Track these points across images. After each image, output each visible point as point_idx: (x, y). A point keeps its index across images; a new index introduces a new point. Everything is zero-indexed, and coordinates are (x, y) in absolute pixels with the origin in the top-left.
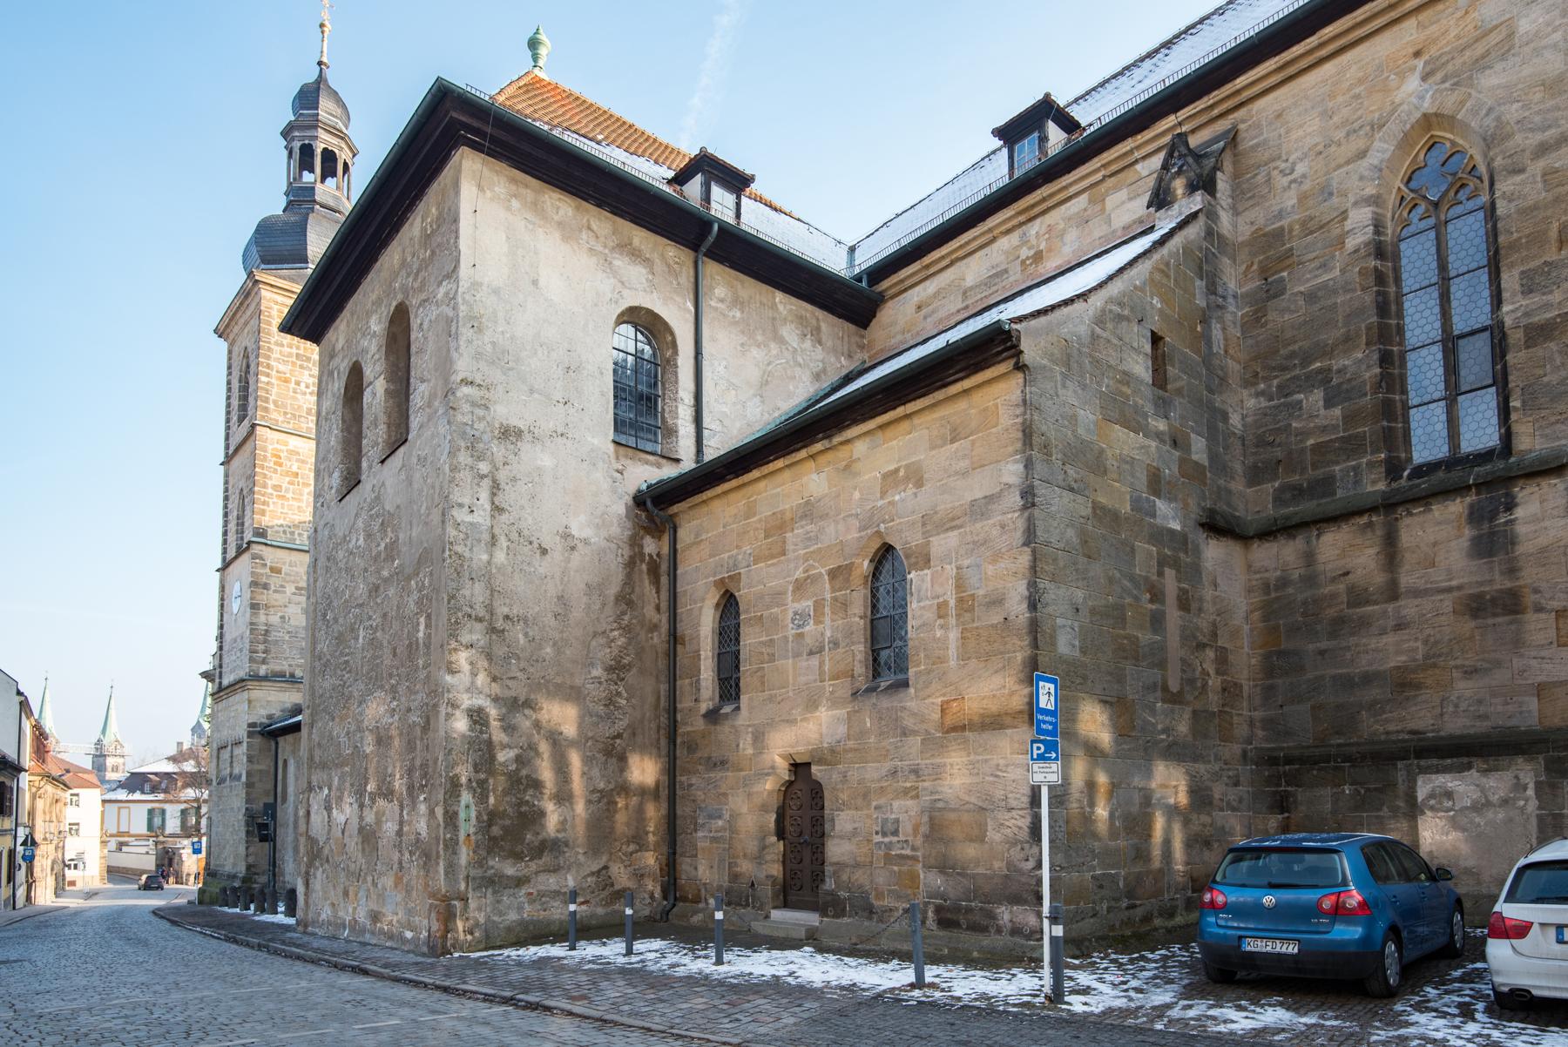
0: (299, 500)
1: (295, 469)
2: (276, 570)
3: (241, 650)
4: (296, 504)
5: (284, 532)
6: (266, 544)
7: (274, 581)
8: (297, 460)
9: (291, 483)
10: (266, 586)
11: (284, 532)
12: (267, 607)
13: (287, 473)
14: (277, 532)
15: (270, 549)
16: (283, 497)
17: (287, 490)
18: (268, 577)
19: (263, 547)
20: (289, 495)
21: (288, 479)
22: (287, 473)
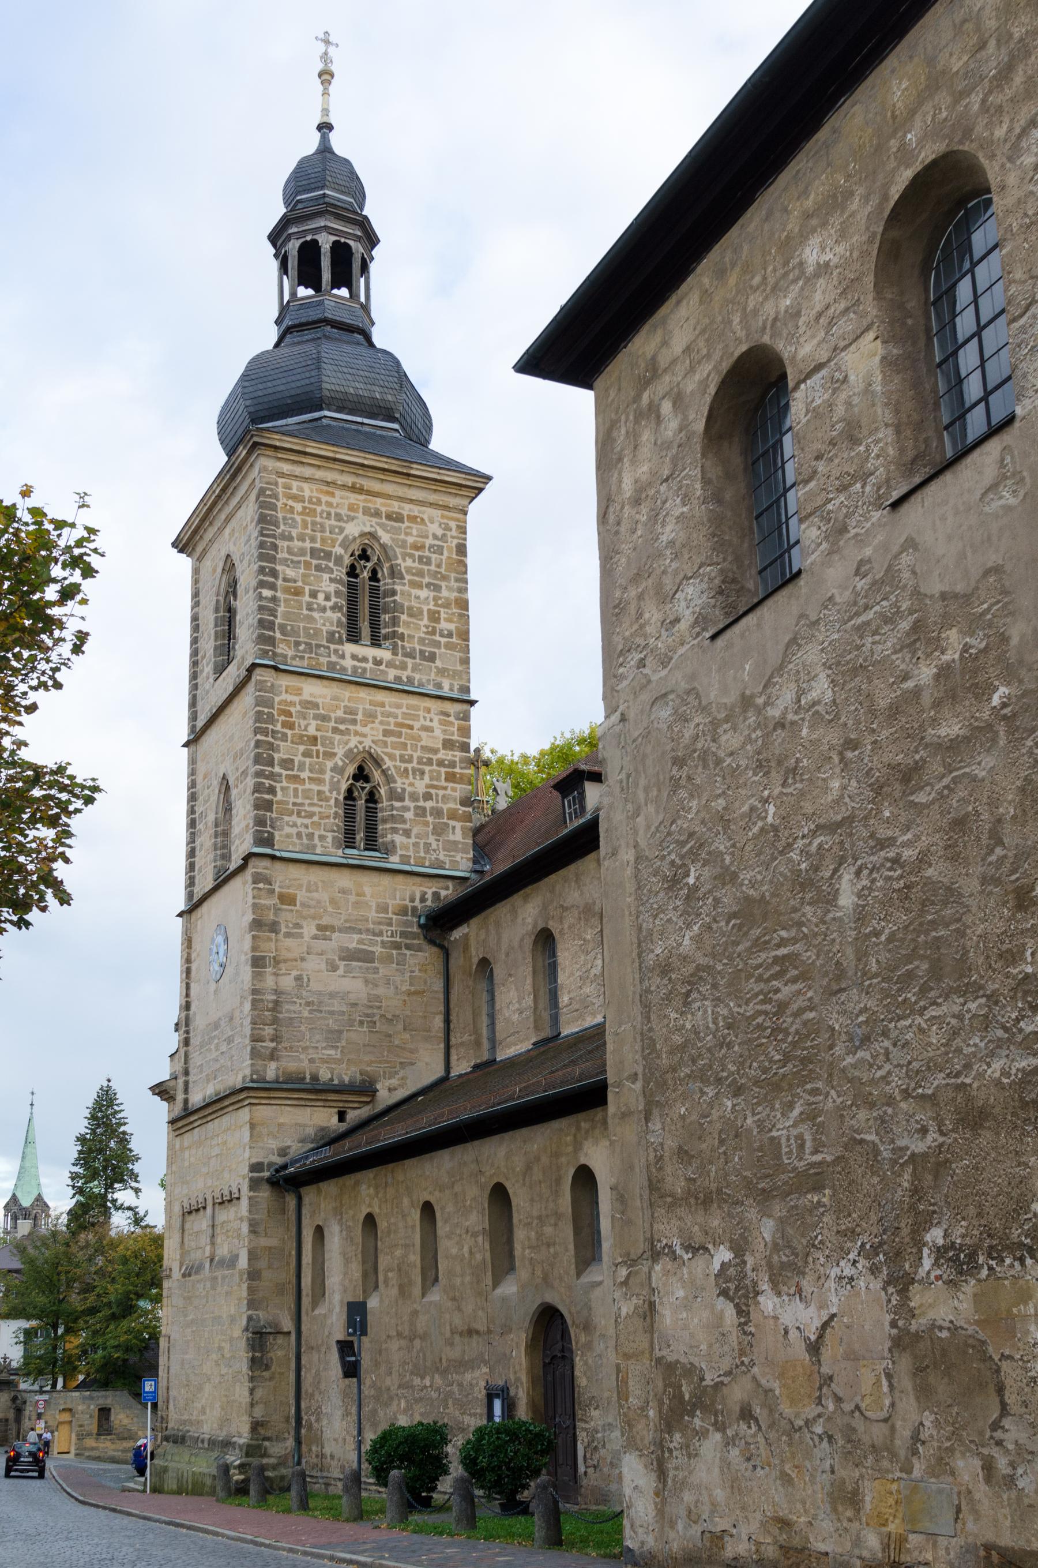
0: (319, 781)
1: (312, 731)
2: (287, 899)
3: (230, 1040)
4: (315, 788)
5: (299, 835)
6: (273, 857)
7: (287, 917)
8: (316, 717)
9: (307, 754)
10: (274, 927)
11: (299, 835)
12: (277, 961)
13: (301, 739)
14: (288, 836)
15: (278, 866)
16: (295, 778)
17: (301, 768)
18: (277, 910)
19: (266, 863)
20: (305, 775)
21: (302, 748)
22: (301, 739)
